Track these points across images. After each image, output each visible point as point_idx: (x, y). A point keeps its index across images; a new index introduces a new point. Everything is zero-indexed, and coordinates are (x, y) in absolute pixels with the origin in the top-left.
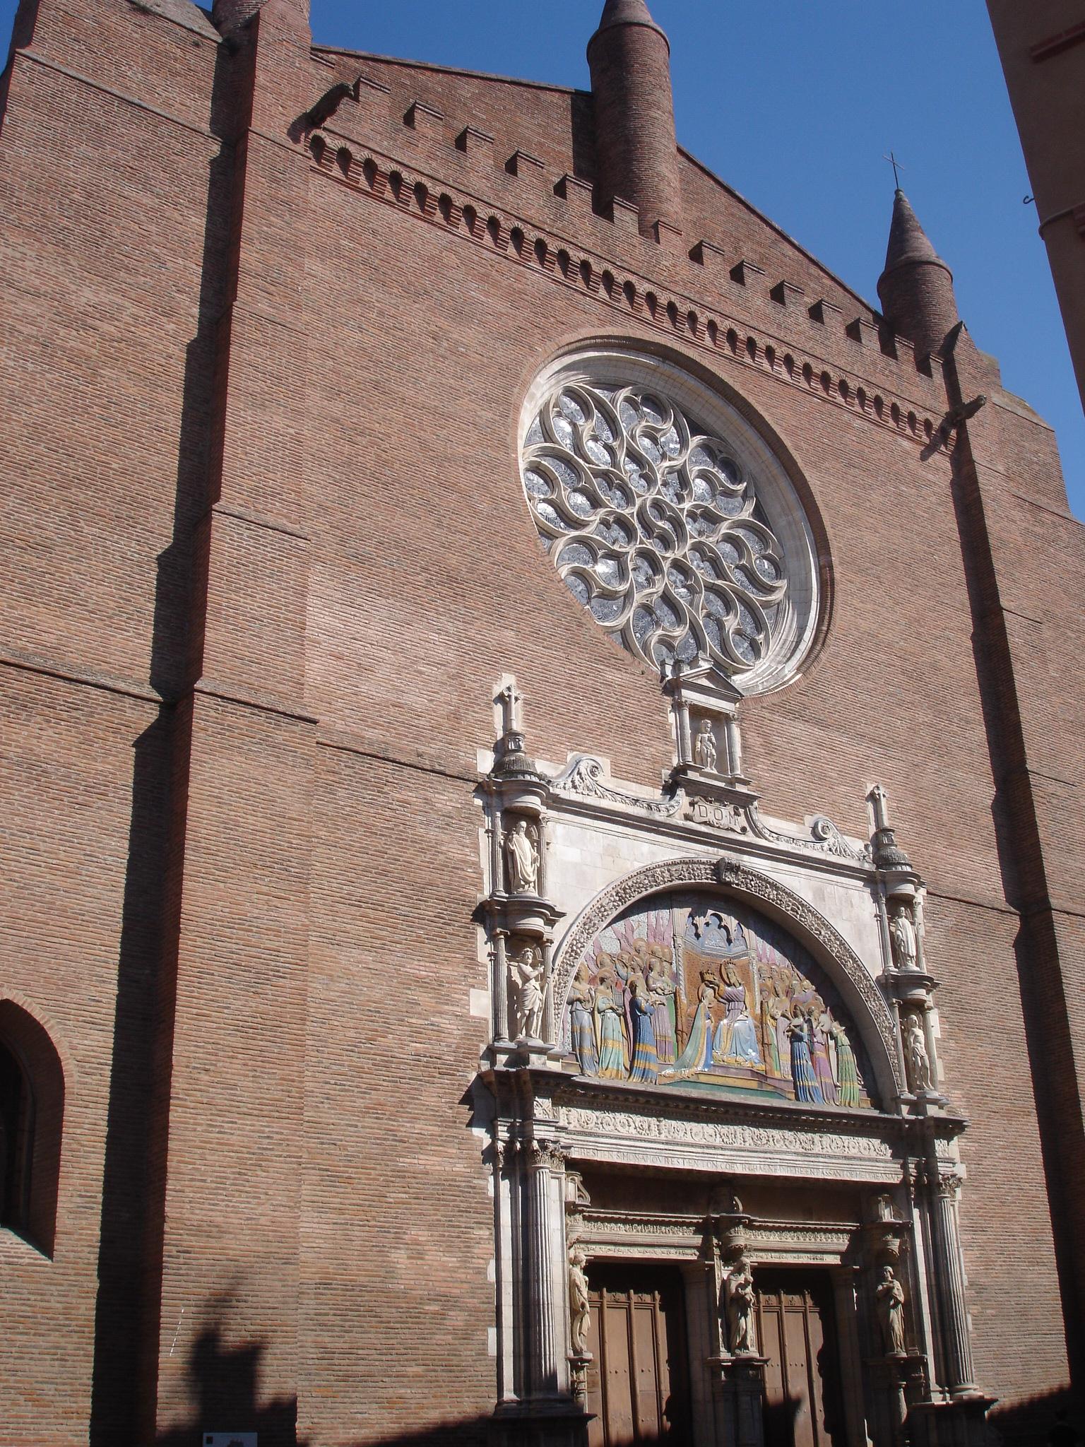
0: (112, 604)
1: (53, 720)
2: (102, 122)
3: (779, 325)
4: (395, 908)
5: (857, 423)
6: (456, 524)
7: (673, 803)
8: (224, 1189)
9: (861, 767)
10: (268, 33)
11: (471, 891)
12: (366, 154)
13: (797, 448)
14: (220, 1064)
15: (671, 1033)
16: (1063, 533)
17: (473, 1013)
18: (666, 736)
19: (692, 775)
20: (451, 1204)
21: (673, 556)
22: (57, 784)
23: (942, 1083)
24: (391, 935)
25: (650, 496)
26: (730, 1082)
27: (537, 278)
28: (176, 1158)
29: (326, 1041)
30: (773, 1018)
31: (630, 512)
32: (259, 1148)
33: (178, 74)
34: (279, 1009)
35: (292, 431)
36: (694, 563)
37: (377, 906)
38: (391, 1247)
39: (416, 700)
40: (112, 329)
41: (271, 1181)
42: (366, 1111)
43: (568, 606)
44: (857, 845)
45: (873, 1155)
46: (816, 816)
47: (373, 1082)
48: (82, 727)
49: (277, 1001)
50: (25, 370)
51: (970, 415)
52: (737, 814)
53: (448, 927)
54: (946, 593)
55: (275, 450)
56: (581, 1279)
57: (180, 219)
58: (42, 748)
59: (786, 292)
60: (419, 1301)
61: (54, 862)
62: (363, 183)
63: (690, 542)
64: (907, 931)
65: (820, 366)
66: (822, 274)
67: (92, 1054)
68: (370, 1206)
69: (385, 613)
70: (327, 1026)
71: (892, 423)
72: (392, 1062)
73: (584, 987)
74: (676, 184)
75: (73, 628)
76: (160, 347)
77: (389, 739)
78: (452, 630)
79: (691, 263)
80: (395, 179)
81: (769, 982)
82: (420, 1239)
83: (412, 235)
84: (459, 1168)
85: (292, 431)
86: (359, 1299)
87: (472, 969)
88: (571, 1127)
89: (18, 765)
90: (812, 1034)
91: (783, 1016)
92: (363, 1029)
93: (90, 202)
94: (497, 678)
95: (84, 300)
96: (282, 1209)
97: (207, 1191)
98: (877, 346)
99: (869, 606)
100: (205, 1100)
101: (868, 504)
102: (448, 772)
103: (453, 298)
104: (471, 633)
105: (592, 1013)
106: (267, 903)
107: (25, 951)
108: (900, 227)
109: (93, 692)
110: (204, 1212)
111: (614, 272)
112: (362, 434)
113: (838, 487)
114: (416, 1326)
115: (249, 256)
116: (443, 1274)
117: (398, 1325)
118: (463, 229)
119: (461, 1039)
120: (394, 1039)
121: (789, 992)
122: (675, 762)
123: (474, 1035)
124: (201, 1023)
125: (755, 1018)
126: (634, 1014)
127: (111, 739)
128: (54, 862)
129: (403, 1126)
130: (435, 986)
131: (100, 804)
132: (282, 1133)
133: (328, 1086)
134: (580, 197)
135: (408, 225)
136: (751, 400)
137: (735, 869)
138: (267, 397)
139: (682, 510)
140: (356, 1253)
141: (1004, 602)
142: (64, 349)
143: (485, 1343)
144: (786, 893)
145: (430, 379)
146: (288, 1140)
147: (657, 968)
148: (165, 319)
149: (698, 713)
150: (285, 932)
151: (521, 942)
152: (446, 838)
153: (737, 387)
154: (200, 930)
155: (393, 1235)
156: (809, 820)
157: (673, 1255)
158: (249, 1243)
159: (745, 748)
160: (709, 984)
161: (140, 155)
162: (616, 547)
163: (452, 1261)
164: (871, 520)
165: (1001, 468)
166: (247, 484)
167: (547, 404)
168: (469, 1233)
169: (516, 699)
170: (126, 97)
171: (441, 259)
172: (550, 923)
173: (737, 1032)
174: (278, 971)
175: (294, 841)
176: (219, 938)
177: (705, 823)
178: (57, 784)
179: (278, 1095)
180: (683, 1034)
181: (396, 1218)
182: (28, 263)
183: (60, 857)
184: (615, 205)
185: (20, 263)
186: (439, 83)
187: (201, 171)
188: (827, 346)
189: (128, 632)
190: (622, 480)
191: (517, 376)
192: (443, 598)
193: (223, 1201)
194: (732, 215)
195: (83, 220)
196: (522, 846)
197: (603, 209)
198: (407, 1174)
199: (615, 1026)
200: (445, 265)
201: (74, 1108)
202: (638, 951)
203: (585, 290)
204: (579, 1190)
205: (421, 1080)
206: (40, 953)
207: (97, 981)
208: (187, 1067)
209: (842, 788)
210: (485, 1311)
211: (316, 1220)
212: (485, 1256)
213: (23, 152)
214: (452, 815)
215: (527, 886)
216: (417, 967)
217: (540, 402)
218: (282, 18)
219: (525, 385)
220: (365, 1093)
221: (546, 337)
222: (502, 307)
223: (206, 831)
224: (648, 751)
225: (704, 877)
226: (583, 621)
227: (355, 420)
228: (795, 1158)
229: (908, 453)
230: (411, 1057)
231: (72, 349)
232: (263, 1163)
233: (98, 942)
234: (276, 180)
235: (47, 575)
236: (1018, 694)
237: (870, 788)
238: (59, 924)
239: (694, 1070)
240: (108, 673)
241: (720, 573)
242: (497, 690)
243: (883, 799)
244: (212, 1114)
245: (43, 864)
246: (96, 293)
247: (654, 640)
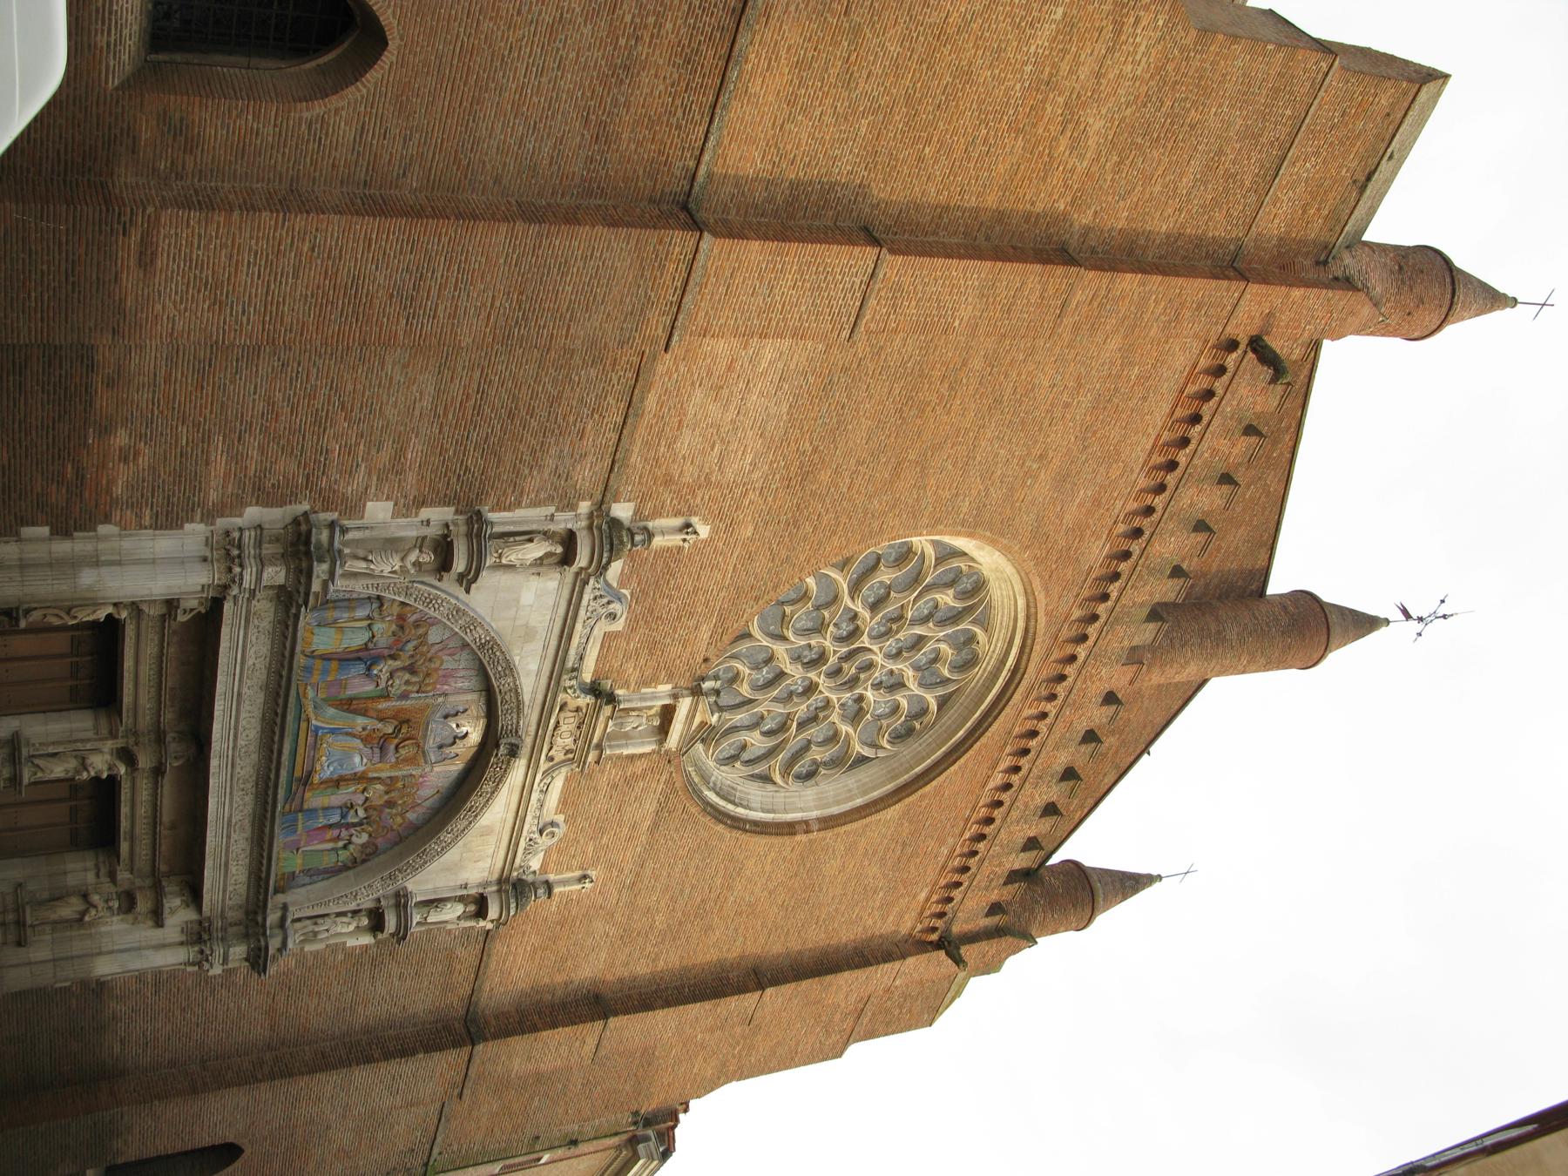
0: (789, 147)
1: (673, 90)
2: (1264, 140)
3: (1041, 778)
4: (475, 427)
5: (945, 851)
6: (860, 478)
7: (578, 692)
8: (190, 268)
9: (610, 866)
10: (1340, 300)
11: (492, 500)
12: (1220, 391)
13: (923, 797)
14: (319, 262)
15: (350, 693)
16: (834, 1038)
17: (369, 504)
18: (646, 684)
19: (607, 710)
20: (176, 488)
21: (821, 682)
22: (609, 93)
23: (302, 949)
24: (448, 423)
25: (879, 659)
26: (301, 751)
27: (1096, 552)
28: (222, 219)
29: (341, 362)
30: (365, 790)
31: (865, 641)
32: (233, 302)
33: (1304, 212)
34: (375, 319)
35: (957, 323)
36: (814, 700)
37: (478, 409)
38: (131, 430)
39: (687, 442)
40: (1062, 148)
41: (199, 314)
42: (270, 403)
43: (775, 587)
44: (535, 863)
45: (230, 888)
46: (562, 825)
47: (300, 409)
48: (665, 119)
49: (384, 316)
50: (1025, 63)
51: (948, 954)
52: (567, 752)
54: (779, 937)
55: (939, 307)
56: (101, 615)
57: (1166, 214)
58: (645, 78)
59: (1072, 783)
60: (77, 459)
61: (529, 91)
62: (1192, 389)
63: (834, 697)
64: (452, 912)
65: (1000, 816)
66: (1086, 811)
67: (331, 130)
68: (174, 409)
69: (772, 412)
70: (357, 362)
71: (943, 882)
72: (320, 427)
73: (396, 610)
74: (1177, 679)
75: (766, 109)
76: (1042, 195)
77: (647, 417)
78: (755, 476)
79: (1104, 694)
80: (1195, 419)
81: (400, 785)
82: (141, 459)
83: (1140, 435)
84: (213, 496)
85: (957, 323)
86: (78, 399)
87: (413, 504)
88: (254, 602)
89: (629, 55)
90: (348, 826)
91: (367, 799)
92: (354, 399)
93: (1186, 128)
94: (705, 521)
95: (1091, 121)
96: (170, 325)
97: (188, 251)
98: (1017, 866)
99: (768, 868)
100: (282, 248)
101: (866, 863)
102: (612, 475)
103: (1078, 473)
104: (751, 495)
105: (368, 618)
106: (484, 305)
107: (438, 63)
108: (1130, 883)
109: (701, 129)
110: (166, 248)
111: (1097, 625)
112: (951, 388)
113: (884, 836)
114: (50, 457)
115: (1128, 283)
116: (104, 482)
117: (51, 437)
118: (1143, 482)
119: (343, 494)
120: (344, 428)
121: (390, 804)
122: (619, 692)
124: (361, 242)
125: (364, 772)
126: (366, 658)
127: (653, 147)
128: (529, 91)
129: (255, 439)
130: (397, 467)
131: (587, 136)
132: (248, 324)
133: (295, 365)
134: (1168, 590)
135: (1150, 430)
136: (971, 752)
137: (513, 752)
138: (991, 300)
139: (866, 689)
140: (125, 396)
141: (770, 991)
142: (1044, 101)
143: (33, 524)
144: (488, 800)
145: (1002, 452)
146: (241, 330)
147: (415, 679)
148: (1069, 199)
149: (667, 713)
150: (453, 324)
151: (443, 551)
152: (546, 476)
153: (983, 740)
154: (457, 241)
155: (143, 431)
156: (560, 818)
157: (127, 699)
158: (134, 294)
159: (632, 758)
160: (397, 730)
161: (1228, 176)
162: (831, 628)
163: (118, 490)
164: (851, 866)
165: (898, 982)
166: (907, 280)
167: (973, 560)
168: (147, 506)
169: (684, 540)
170: (1285, 163)
171: (1116, 461)
172: (461, 578)
173: (351, 757)
174: (413, 318)
175: (545, 331)
176: (448, 258)
177: (558, 722)
178: (609, 93)
179: (288, 320)
180: (349, 705)
181: (162, 434)
182: (1130, 67)
183: (534, 98)
184: (1160, 624)
185: (1130, 59)
186: (1282, 454)
187: (1211, 235)
188: (1018, 822)
189: (761, 163)
190: (897, 632)
191: (1003, 535)
192: (786, 467)
193: (179, 267)
194: (1145, 727)
195: (1169, 121)
196: (536, 550)
197: (1156, 614)
198: (206, 445)
199: (357, 640)
200: (1110, 467)
201: (273, 113)
202: (430, 660)
203: (1081, 597)
204: (192, 610)
205: (301, 455)
206: (435, 78)
207: (406, 135)
208: (317, 230)
209: (591, 848)
210: (67, 523)
211: (159, 355)
212: (123, 523)
213: (1238, 63)
215: (495, 555)
216: (415, 451)
217: (975, 554)
218: (1352, 313)
219: (993, 542)
220: (289, 400)
221: (1039, 561)
222: (1069, 519)
223: (557, 243)
224: (629, 667)
225: (504, 721)
226: (760, 602)
227: (964, 381)
228: (226, 815)
229: (914, 897)
230: (324, 445)
231: (1044, 109)
232: (217, 307)
233: (445, 136)
234: (1199, 308)
235: (819, 84)
236: (681, 1007)
237: (593, 873)
238: (465, 96)
239: (312, 716)
240: (719, 144)
241: (802, 725)
242: (694, 520)
243: (580, 886)
244: (267, 255)
245: (526, 81)
246: (1098, 133)
247: (740, 667)
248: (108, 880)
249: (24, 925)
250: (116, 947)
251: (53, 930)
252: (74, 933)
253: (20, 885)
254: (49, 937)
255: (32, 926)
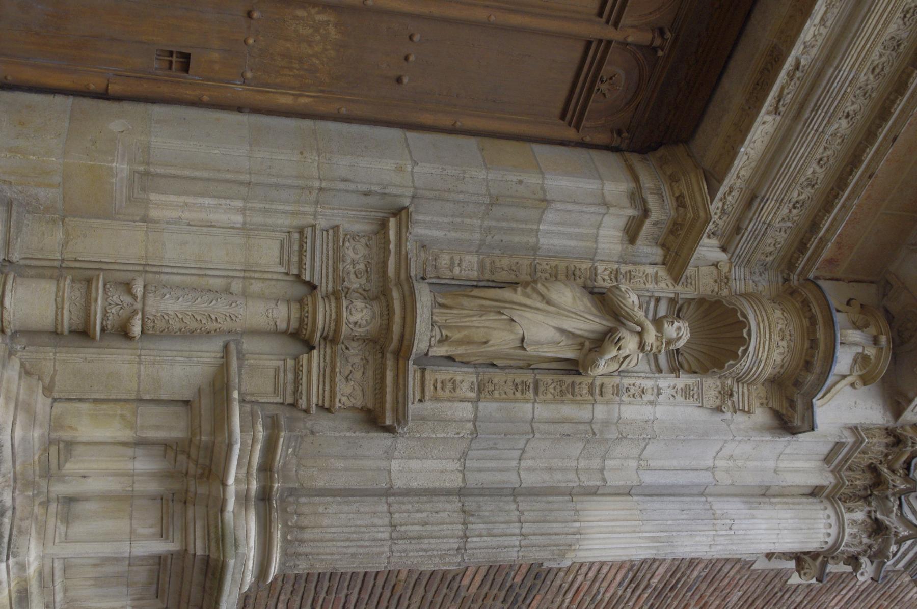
248: (657, 253)
249: (402, 352)
250: (649, 478)
251: (482, 390)
252: (543, 411)
253: (399, 212)
254: (465, 410)
255: (425, 360)
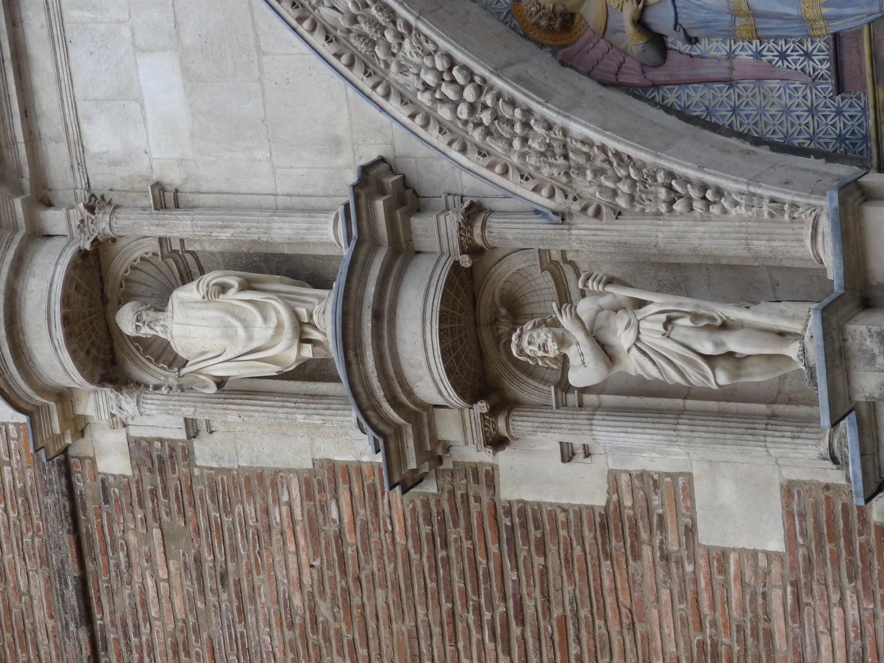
17: (776, 544)
53: (529, 611)
87: (634, 527)
123: (849, 543)
214: (190, 561)
